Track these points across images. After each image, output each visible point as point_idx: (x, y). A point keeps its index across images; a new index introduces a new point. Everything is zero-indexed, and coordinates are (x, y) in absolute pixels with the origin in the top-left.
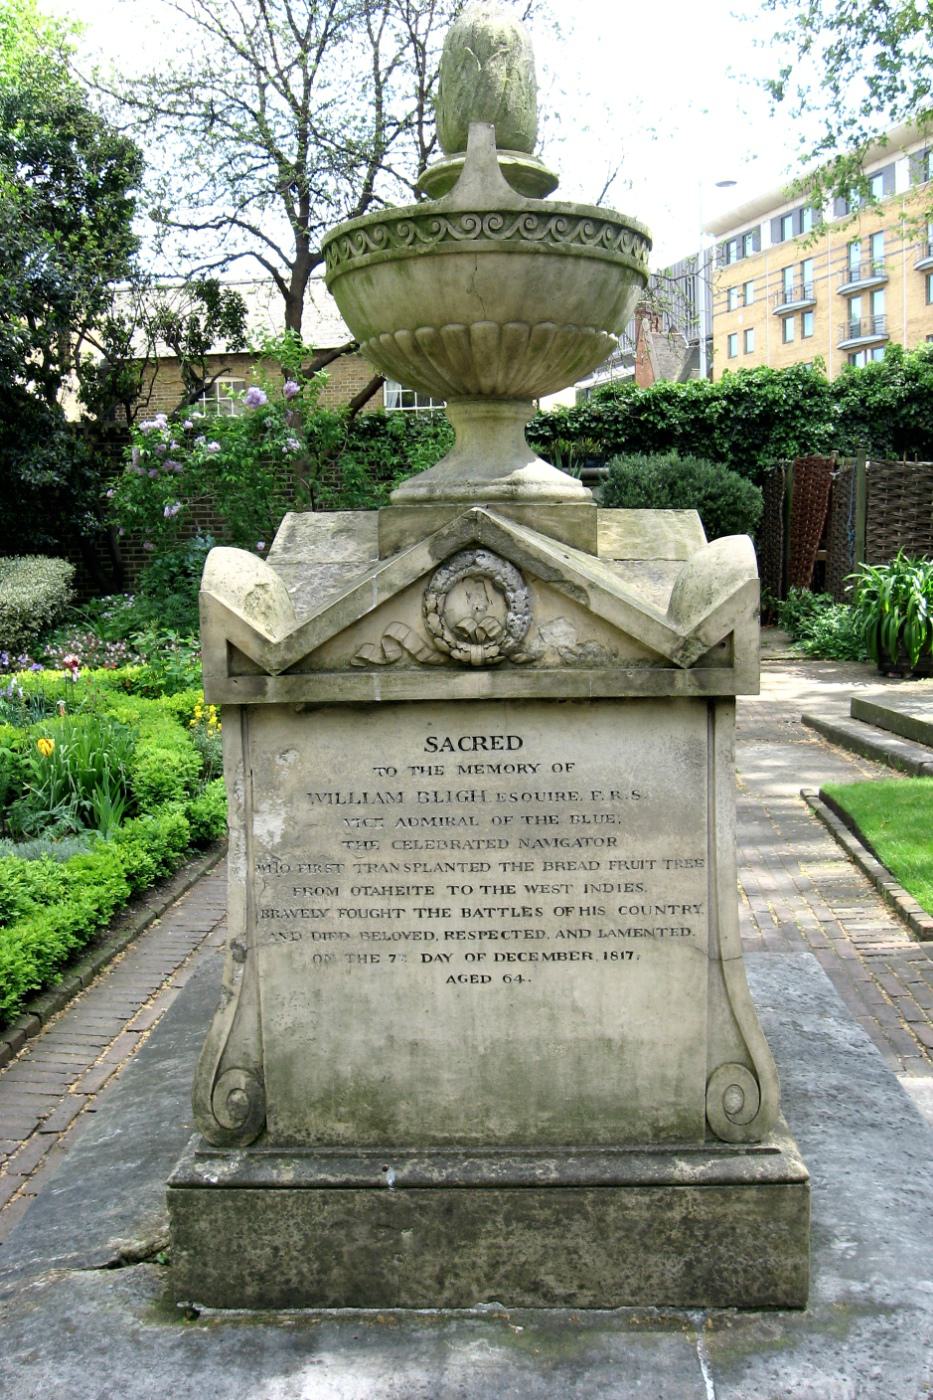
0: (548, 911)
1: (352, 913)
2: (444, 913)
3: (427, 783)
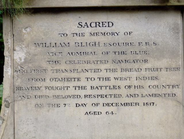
0: (123, 87)
1: (50, 88)
2: (84, 88)
3: (78, 39)
